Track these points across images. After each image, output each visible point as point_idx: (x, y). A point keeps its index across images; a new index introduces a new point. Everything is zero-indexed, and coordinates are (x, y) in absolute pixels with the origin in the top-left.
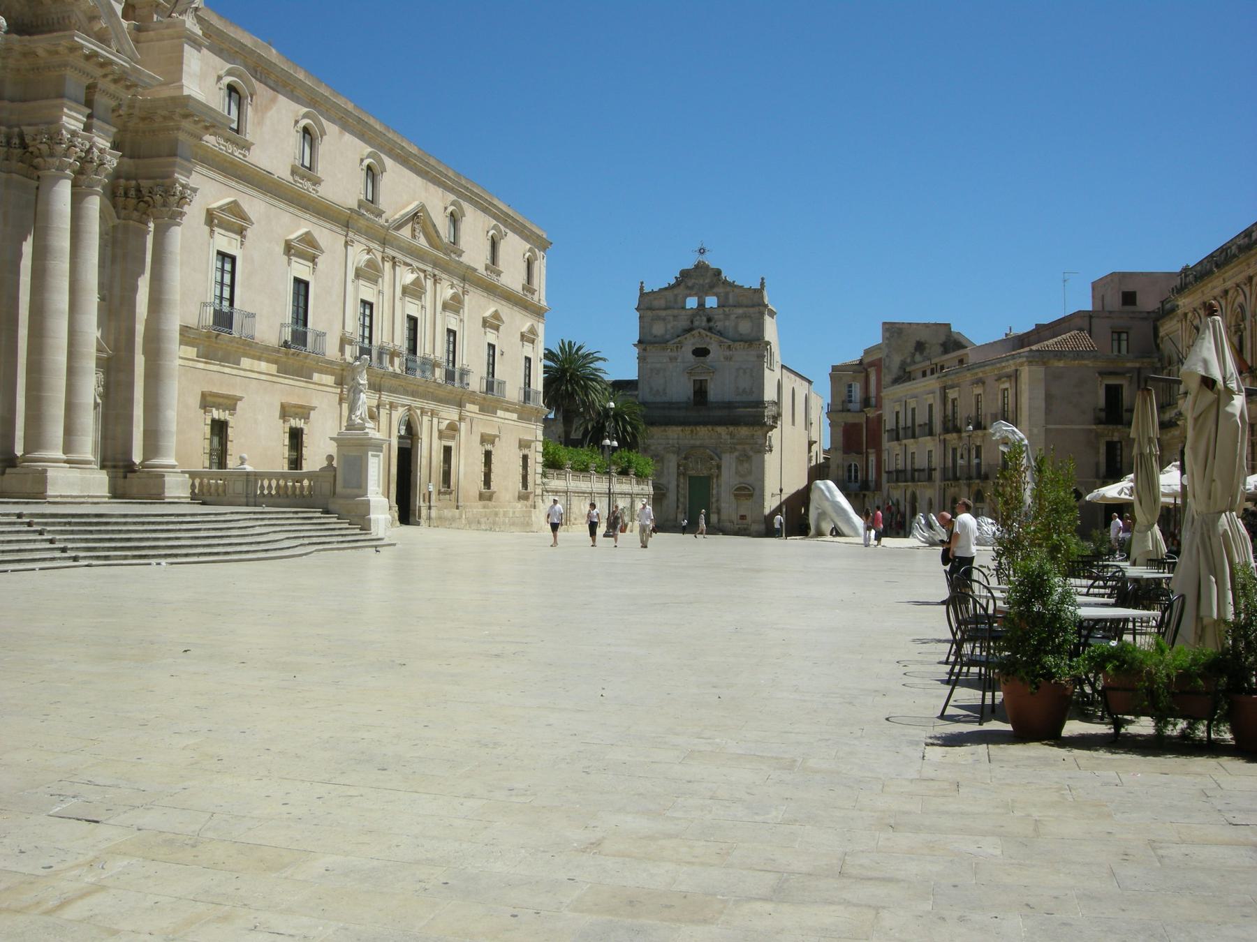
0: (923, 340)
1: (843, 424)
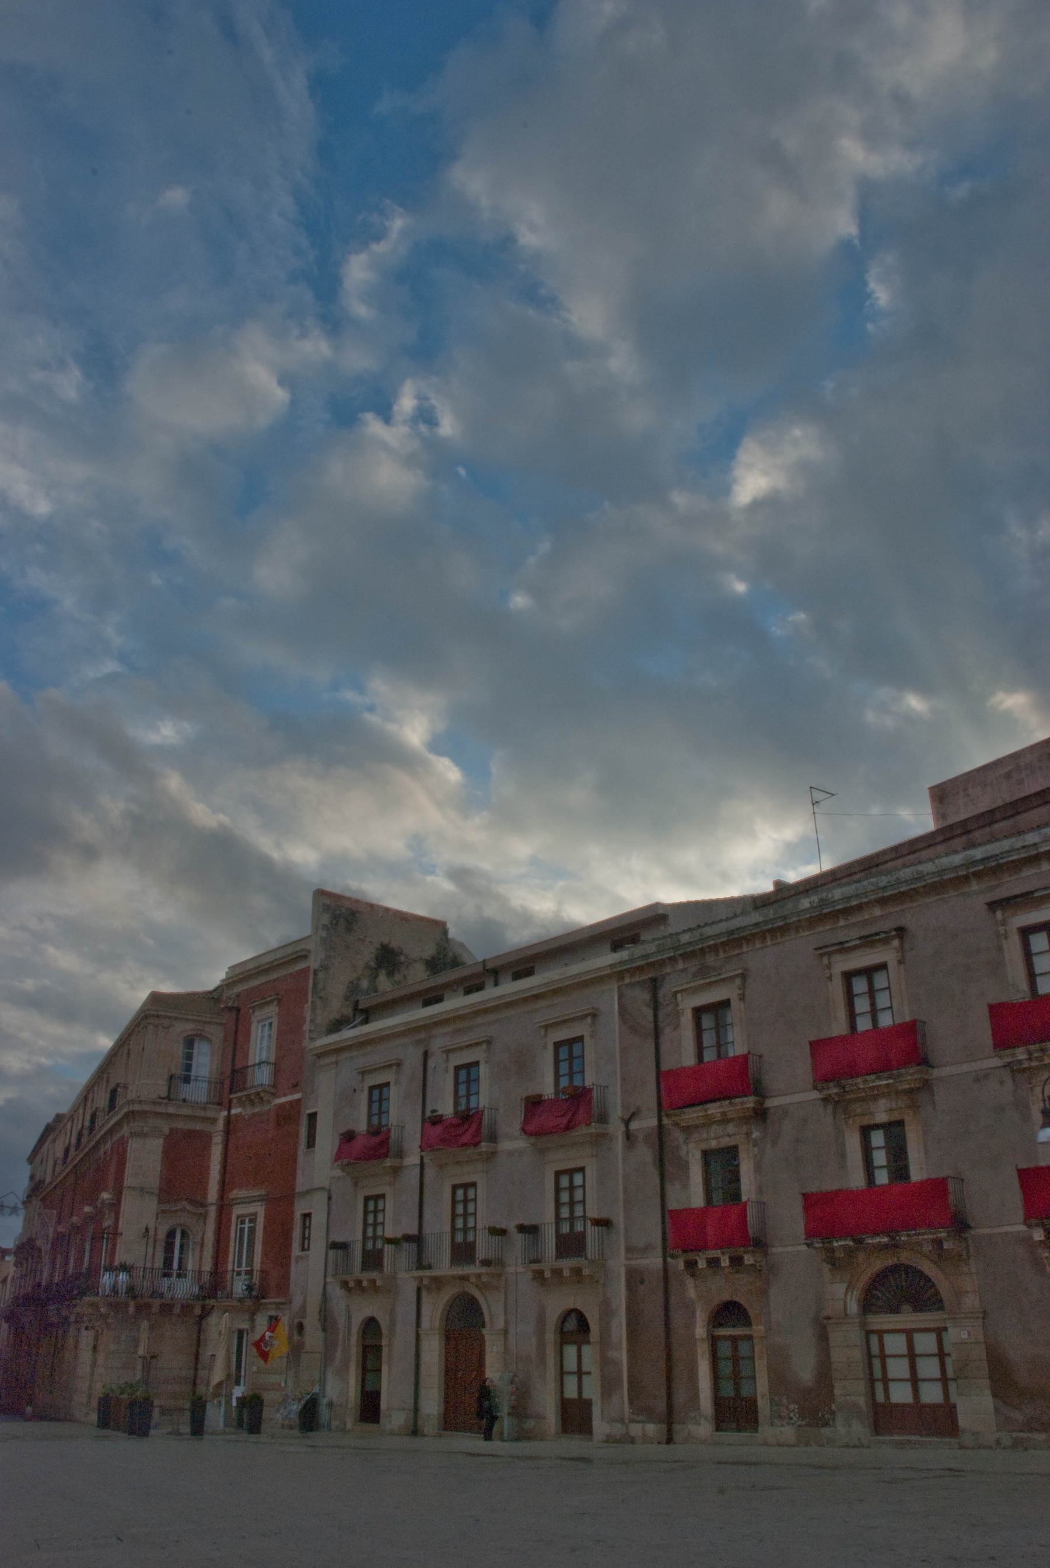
0: (394, 945)
1: (167, 1131)
